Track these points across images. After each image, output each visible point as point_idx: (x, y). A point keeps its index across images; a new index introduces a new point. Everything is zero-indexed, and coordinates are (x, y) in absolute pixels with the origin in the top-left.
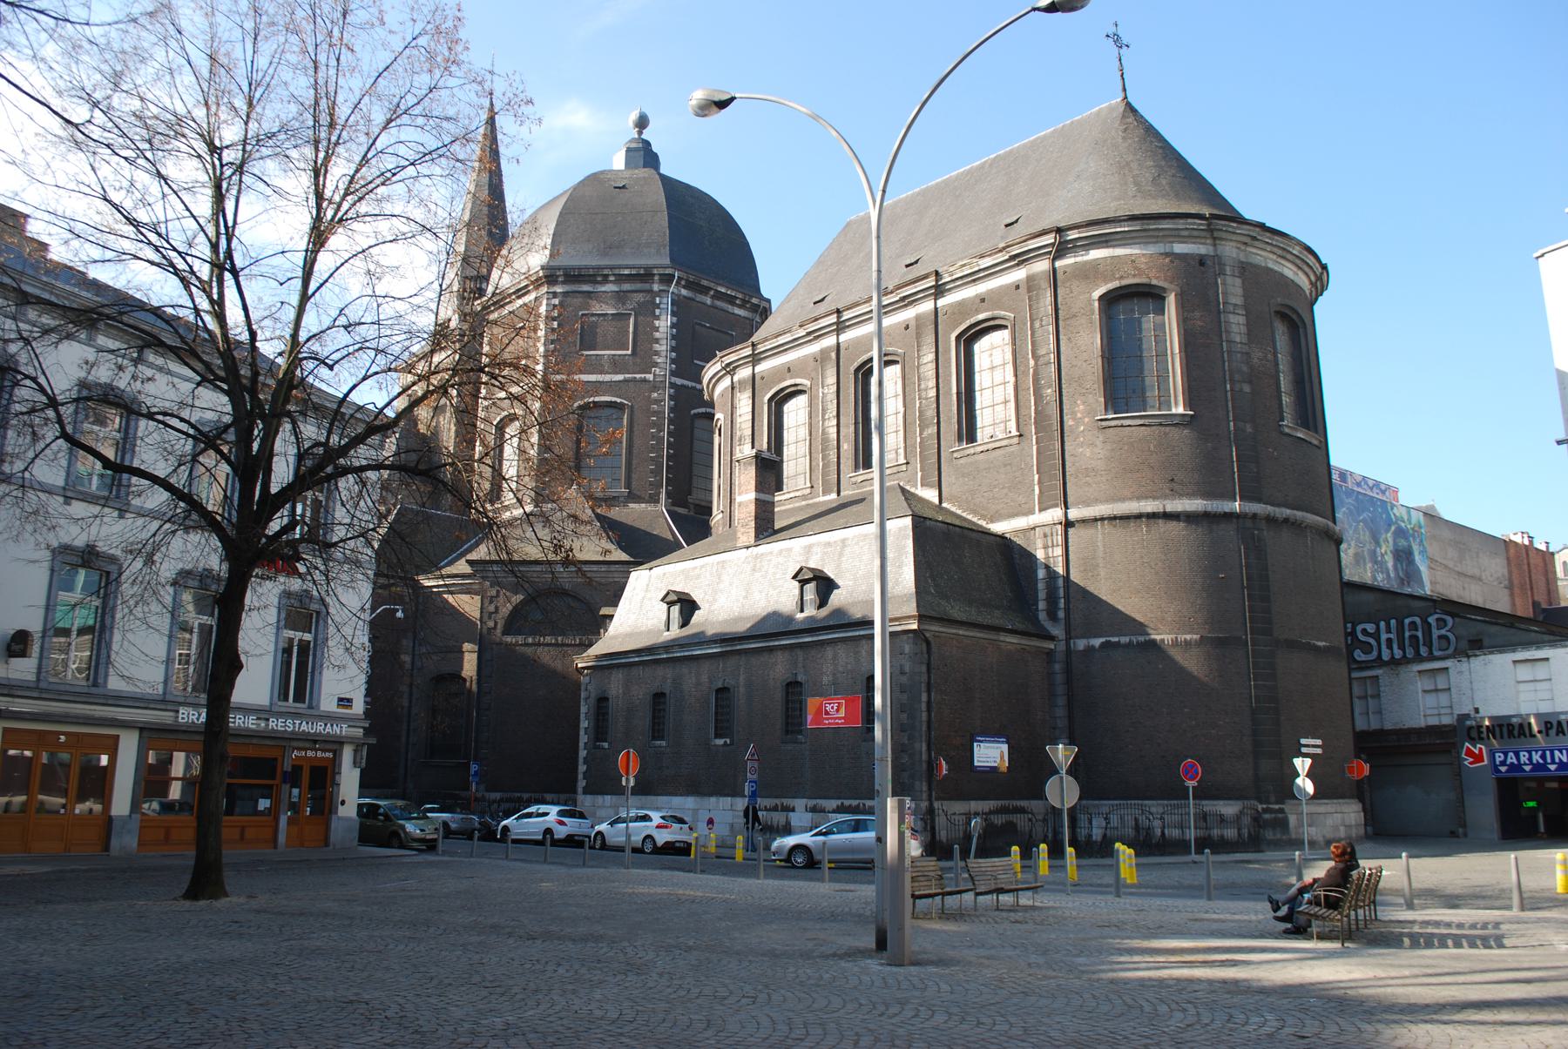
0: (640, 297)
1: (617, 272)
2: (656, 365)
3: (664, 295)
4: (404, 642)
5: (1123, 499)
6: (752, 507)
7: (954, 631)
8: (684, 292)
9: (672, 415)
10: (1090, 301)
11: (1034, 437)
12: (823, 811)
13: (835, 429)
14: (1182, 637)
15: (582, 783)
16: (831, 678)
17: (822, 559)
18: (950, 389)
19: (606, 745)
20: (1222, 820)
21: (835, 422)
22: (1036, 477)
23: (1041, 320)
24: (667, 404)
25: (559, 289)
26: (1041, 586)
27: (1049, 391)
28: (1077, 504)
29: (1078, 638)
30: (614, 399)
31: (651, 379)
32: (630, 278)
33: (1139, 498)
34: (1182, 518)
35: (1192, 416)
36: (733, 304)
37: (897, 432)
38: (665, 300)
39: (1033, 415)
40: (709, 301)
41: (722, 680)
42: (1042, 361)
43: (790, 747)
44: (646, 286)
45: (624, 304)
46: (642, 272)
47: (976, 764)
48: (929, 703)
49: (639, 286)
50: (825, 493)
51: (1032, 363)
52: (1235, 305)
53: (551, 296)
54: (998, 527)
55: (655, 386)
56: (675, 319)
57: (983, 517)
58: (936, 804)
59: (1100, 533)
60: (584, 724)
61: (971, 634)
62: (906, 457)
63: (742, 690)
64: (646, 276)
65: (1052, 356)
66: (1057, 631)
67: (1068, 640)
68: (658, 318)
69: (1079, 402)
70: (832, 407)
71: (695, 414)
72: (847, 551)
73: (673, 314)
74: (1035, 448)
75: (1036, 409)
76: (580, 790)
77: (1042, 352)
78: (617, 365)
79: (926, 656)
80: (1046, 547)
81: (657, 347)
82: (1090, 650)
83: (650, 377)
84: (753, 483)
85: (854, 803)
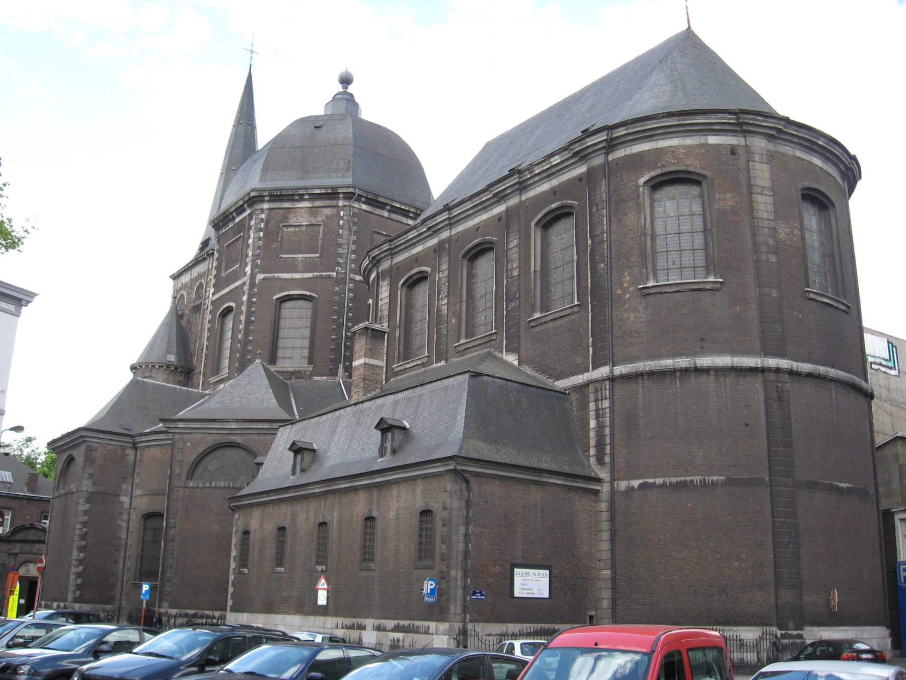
1: (310, 191)
2: (339, 264)
4: (124, 486)
8: (364, 207)
9: (350, 305)
10: (637, 187)
11: (590, 305)
12: (385, 630)
15: (230, 603)
19: (246, 571)
20: (742, 644)
23: (598, 205)
25: (266, 206)
26: (592, 434)
27: (602, 265)
29: (619, 479)
30: (304, 293)
32: (320, 196)
35: (721, 283)
36: (407, 217)
39: (589, 286)
40: (386, 214)
41: (322, 516)
42: (597, 240)
43: (365, 574)
44: (333, 203)
45: (315, 217)
46: (330, 191)
48: (466, 535)
49: (327, 203)
50: (438, 361)
51: (589, 242)
52: (763, 188)
57: (551, 376)
58: (470, 626)
60: (234, 553)
63: (335, 524)
65: (605, 235)
66: (604, 474)
67: (612, 481)
69: (626, 274)
74: (590, 314)
76: (228, 608)
77: (598, 232)
80: (596, 401)
81: (340, 251)
82: (630, 489)
85: (406, 623)
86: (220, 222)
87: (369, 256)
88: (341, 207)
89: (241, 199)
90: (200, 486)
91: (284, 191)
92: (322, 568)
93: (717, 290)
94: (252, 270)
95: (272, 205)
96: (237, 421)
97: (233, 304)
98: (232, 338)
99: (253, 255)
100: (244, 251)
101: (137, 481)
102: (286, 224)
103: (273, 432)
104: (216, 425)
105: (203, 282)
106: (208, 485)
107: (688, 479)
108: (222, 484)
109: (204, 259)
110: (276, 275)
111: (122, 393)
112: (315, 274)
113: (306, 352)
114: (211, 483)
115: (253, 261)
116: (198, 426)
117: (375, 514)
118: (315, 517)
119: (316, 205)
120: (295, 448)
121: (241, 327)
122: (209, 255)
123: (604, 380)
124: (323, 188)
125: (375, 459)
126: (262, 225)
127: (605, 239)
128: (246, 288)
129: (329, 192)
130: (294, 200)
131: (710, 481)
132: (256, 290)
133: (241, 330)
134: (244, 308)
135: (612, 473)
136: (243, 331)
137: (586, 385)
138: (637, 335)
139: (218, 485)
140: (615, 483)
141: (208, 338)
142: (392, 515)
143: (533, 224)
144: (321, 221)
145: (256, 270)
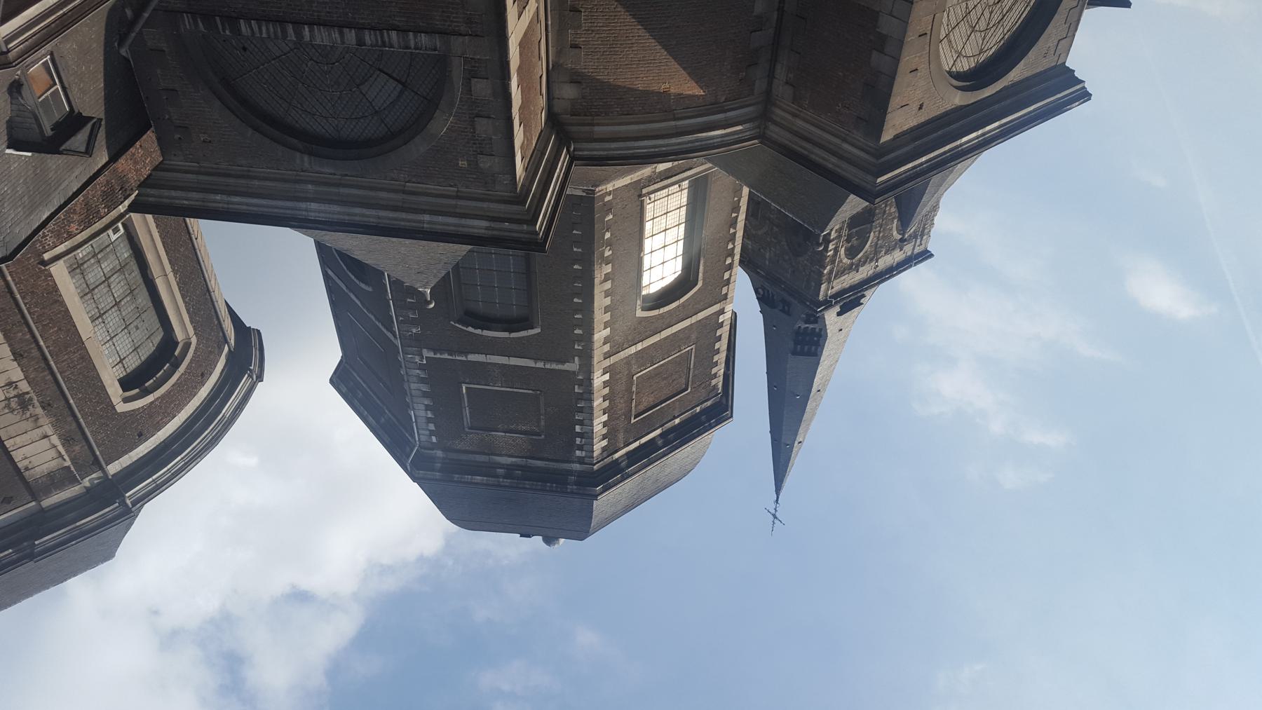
2: (421, 367)
25: (576, 467)
30: (478, 331)
38: (423, 438)
53: (587, 460)
94: (589, 380)
104: (371, 216)
106: (368, 37)
108: (322, 37)
110: (540, 365)
112: (464, 358)
114: (360, 42)
116: (427, 217)
126: (578, 441)
129: (457, 476)
132: (576, 347)
145: (580, 377)
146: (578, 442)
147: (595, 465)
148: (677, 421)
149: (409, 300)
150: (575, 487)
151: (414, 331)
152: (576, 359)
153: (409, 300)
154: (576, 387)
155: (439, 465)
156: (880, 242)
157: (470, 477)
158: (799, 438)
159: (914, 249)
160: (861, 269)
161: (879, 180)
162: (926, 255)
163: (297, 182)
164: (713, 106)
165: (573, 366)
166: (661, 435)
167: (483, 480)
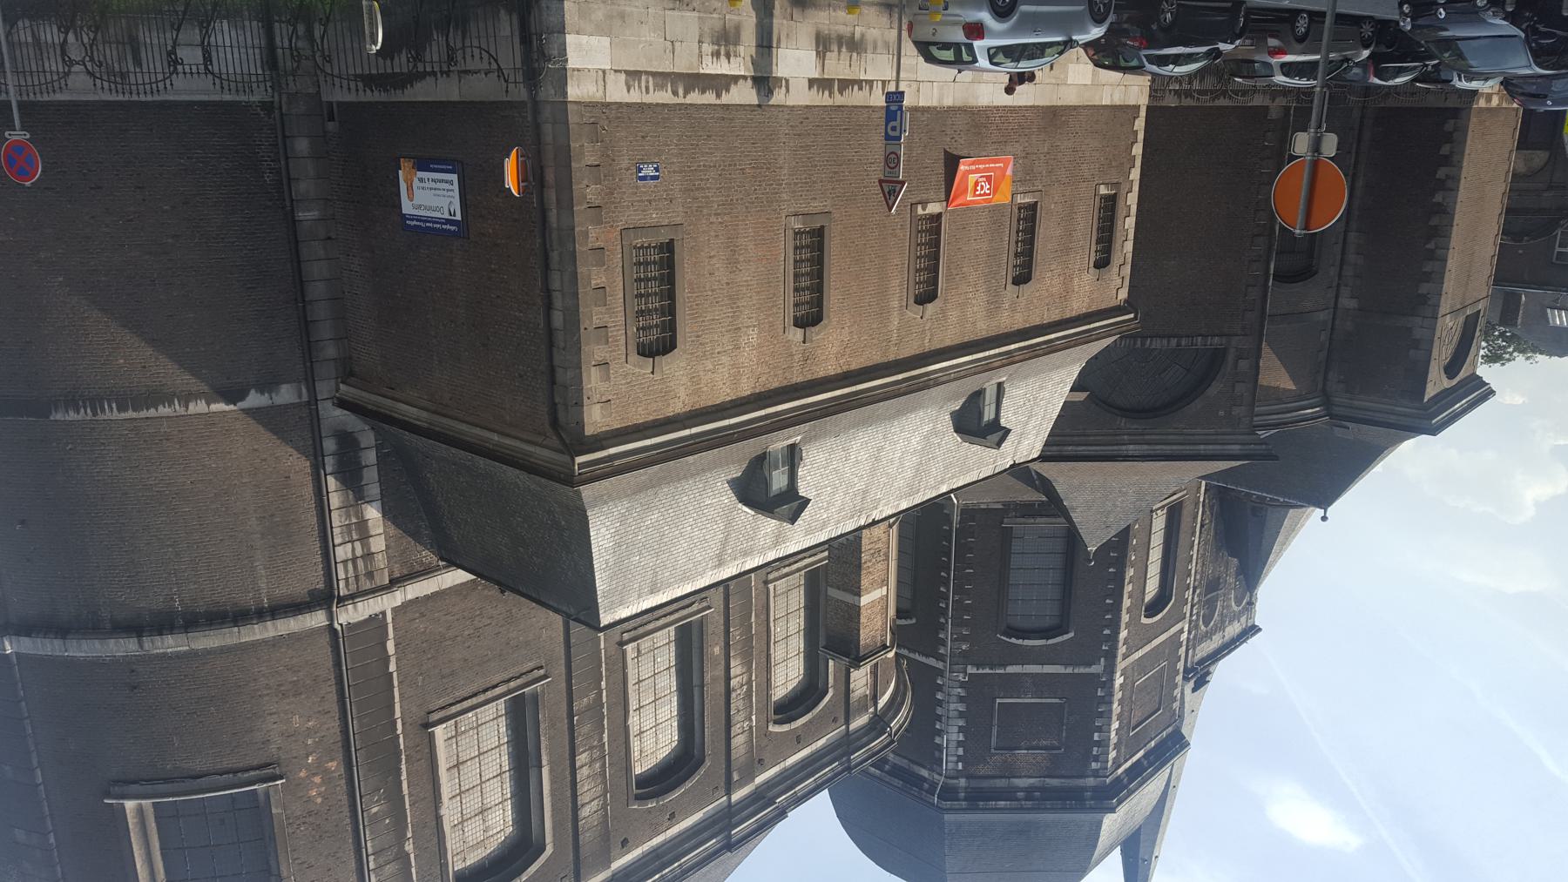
0: (983, 770)
2: (962, 685)
3: (952, 773)
5: (224, 650)
6: (865, 582)
7: (508, 441)
8: (925, 773)
9: (942, 620)
11: (399, 731)
13: (733, 672)
14: (85, 415)
15: (1140, 124)
16: (743, 340)
17: (756, 530)
18: (551, 771)
19: (1103, 190)
21: (733, 683)
22: (392, 667)
24: (948, 634)
25: (1091, 781)
27: (374, 810)
28: (313, 633)
30: (1020, 642)
31: (969, 667)
33: (193, 655)
34: (108, 626)
37: (639, 682)
38: (951, 766)
39: (403, 767)
41: (927, 316)
42: (390, 855)
43: (816, 206)
44: (974, 783)
47: (454, 177)
49: (985, 784)
51: (409, 847)
54: (459, 577)
55: (966, 658)
56: (937, 740)
59: (266, 590)
60: (1130, 223)
61: (477, 431)
62: (624, 653)
64: (978, 798)
65: (372, 866)
66: (333, 415)
67: (314, 400)
68: (960, 744)
70: (737, 702)
71: (911, 619)
72: (714, 549)
73: (939, 748)
74: (398, 714)
75: (399, 775)
76: (1143, 113)
78: (1014, 684)
79: (557, 400)
80: (368, 556)
81: (962, 707)
82: (266, 386)
83: (971, 670)
84: (863, 620)
85: (695, 98)
86: (1175, 744)
87: (890, 735)
88: (962, 777)
89: (1134, 792)
90: (1200, 339)
91: (1059, 806)
92: (924, 209)
93: (116, 782)
94: (1112, 680)
95: (1081, 782)
96: (1126, 458)
97: (1144, 620)
98: (1147, 566)
99: (1111, 703)
100: (1126, 708)
101: (1324, 337)
102: (1054, 752)
103: (1057, 438)
104: (1167, 449)
105: (1203, 627)
107: (130, 414)
109: (1202, 662)
110: (1069, 670)
111: (1343, 491)
112: (1002, 671)
113: (1016, 546)
115: (1111, 694)
116: (1202, 447)
117: (798, 334)
118: (943, 311)
119: (1003, 780)
120: (995, 437)
121: (1128, 588)
122: (1193, 669)
123: (352, 597)
124: (992, 809)
125: (806, 440)
127: (371, 858)
128: (1122, 650)
129: (982, 803)
130: (1042, 789)
131: (82, 410)
132: (1104, 648)
133: (1129, 584)
134: (1125, 618)
135: (315, 419)
136: (1127, 581)
137: (395, 583)
138: (282, 688)
139: (1165, 342)
140: (305, 398)
141: (1191, 561)
142: (753, 336)
143: (549, 850)
144: (994, 755)
146: (1094, 753)
147: (1107, 777)
148: (1153, 743)
149: (965, 617)
150: (1092, 802)
151: (964, 647)
152: (1102, 660)
153: (965, 617)
154: (1099, 689)
155: (963, 794)
156: (1225, 611)
157: (994, 803)
158: (1156, 854)
159: (1247, 621)
160: (1214, 638)
161: (1434, 422)
162: (1253, 630)
163: (1116, 435)
164: (1300, 398)
165: (1096, 669)
166: (1144, 756)
167: (1006, 805)
